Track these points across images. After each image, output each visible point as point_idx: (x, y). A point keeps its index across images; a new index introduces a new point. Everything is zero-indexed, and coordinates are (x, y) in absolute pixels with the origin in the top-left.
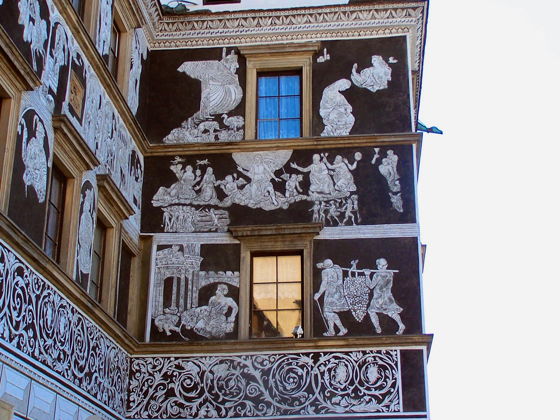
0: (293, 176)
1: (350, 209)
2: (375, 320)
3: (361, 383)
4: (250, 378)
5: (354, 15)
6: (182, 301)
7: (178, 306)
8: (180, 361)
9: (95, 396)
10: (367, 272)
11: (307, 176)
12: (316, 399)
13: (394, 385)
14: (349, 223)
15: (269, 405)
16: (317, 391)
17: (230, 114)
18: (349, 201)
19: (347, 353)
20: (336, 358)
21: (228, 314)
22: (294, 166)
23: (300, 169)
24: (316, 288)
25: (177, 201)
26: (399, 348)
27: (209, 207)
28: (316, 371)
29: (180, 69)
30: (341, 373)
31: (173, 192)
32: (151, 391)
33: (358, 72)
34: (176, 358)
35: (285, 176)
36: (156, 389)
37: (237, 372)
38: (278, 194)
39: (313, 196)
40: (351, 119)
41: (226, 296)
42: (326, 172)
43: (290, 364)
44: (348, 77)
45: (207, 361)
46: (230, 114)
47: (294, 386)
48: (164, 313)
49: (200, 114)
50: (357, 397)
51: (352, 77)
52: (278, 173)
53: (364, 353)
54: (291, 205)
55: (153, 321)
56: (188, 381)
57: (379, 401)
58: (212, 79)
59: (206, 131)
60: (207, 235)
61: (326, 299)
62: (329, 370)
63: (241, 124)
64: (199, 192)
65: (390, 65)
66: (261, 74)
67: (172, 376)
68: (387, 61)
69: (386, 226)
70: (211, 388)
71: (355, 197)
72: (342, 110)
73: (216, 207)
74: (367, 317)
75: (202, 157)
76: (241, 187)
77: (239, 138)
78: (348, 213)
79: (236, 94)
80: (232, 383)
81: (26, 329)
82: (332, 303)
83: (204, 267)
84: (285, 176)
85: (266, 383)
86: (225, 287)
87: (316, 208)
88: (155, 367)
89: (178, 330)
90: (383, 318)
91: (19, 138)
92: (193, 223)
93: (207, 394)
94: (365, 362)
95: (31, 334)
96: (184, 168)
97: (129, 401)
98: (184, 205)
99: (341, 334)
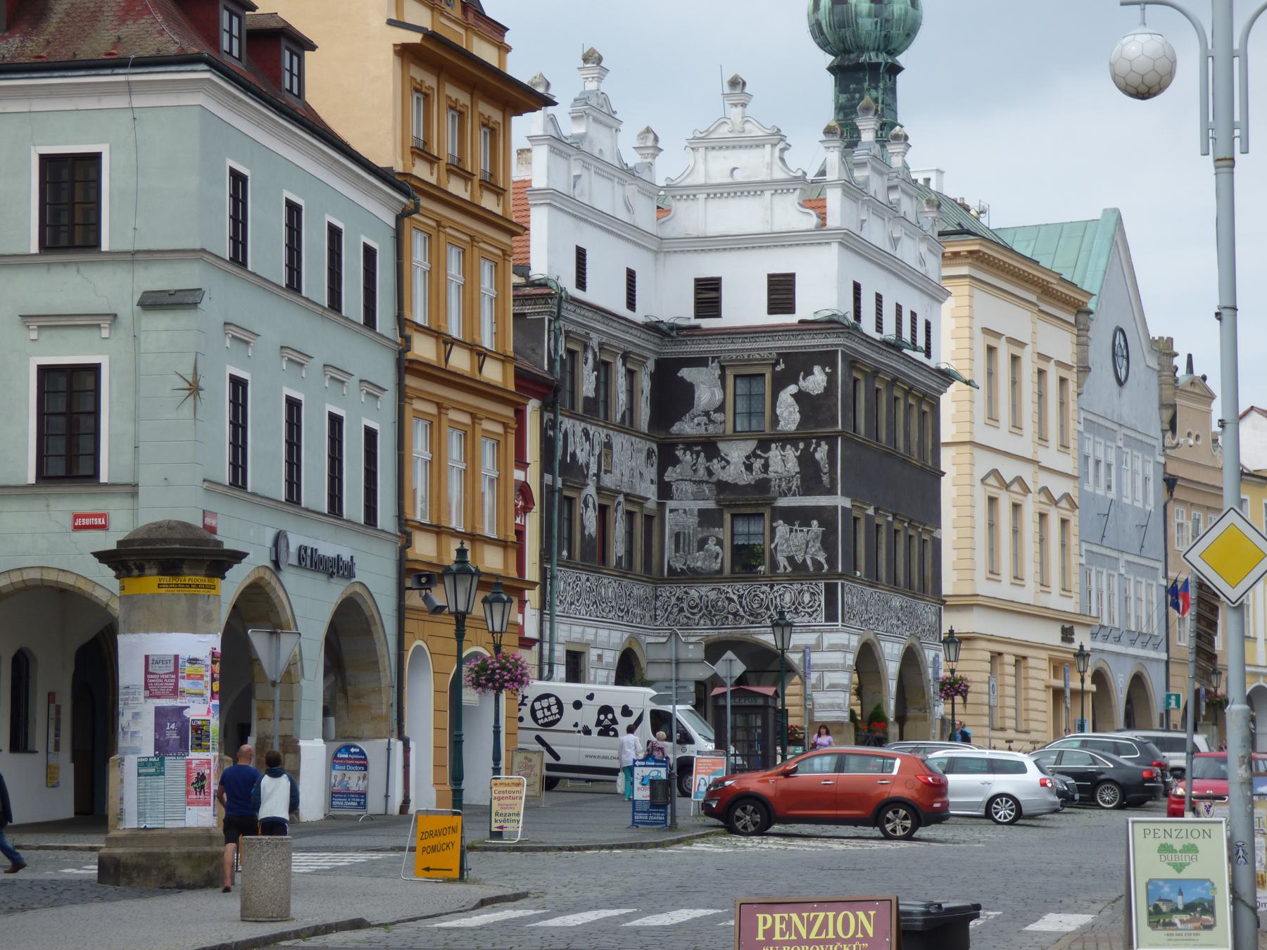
0: (758, 460)
1: (795, 485)
2: (809, 562)
3: (800, 605)
4: (730, 600)
5: (800, 337)
6: (687, 548)
7: (684, 551)
8: (686, 589)
9: (632, 622)
10: (805, 529)
11: (767, 459)
12: (772, 614)
13: (819, 606)
14: (794, 495)
15: (742, 617)
16: (772, 609)
17: (716, 411)
18: (795, 479)
19: (791, 584)
20: (784, 587)
21: (716, 558)
22: (759, 452)
23: (763, 455)
24: (772, 540)
25: (681, 478)
26: (823, 582)
27: (702, 482)
28: (772, 596)
29: (679, 374)
30: (787, 598)
31: (678, 471)
32: (669, 609)
33: (804, 379)
34: (684, 587)
35: (752, 460)
36: (672, 607)
37: (723, 596)
38: (748, 473)
39: (771, 475)
40: (797, 417)
41: (716, 545)
42: (780, 457)
43: (755, 591)
44: (796, 383)
45: (704, 589)
46: (716, 411)
47: (758, 605)
48: (676, 556)
49: (694, 411)
50: (797, 613)
51: (800, 384)
52: (748, 458)
53: (802, 584)
54: (756, 481)
55: (669, 562)
56: (692, 602)
57: (810, 616)
58: (702, 382)
59: (699, 424)
60: (701, 502)
61: (779, 548)
62: (780, 595)
63: (723, 419)
64: (695, 471)
65: (827, 374)
66: (736, 377)
67: (682, 599)
68: (824, 370)
69: (818, 497)
70: (707, 607)
71: (798, 475)
72: (792, 409)
73: (707, 482)
74: (804, 560)
75: (697, 444)
76: (723, 468)
77: (721, 431)
78: (794, 488)
79: (719, 395)
80: (720, 603)
82: (782, 551)
83: (700, 524)
84: (752, 460)
85: (741, 603)
86: (714, 538)
87: (773, 483)
88: (671, 593)
89: (685, 568)
90: (814, 561)
91: (582, 515)
92: (692, 493)
93: (704, 610)
94: (802, 590)
95: (595, 606)
96: (684, 453)
97: (656, 615)
98: (686, 480)
99: (788, 571)
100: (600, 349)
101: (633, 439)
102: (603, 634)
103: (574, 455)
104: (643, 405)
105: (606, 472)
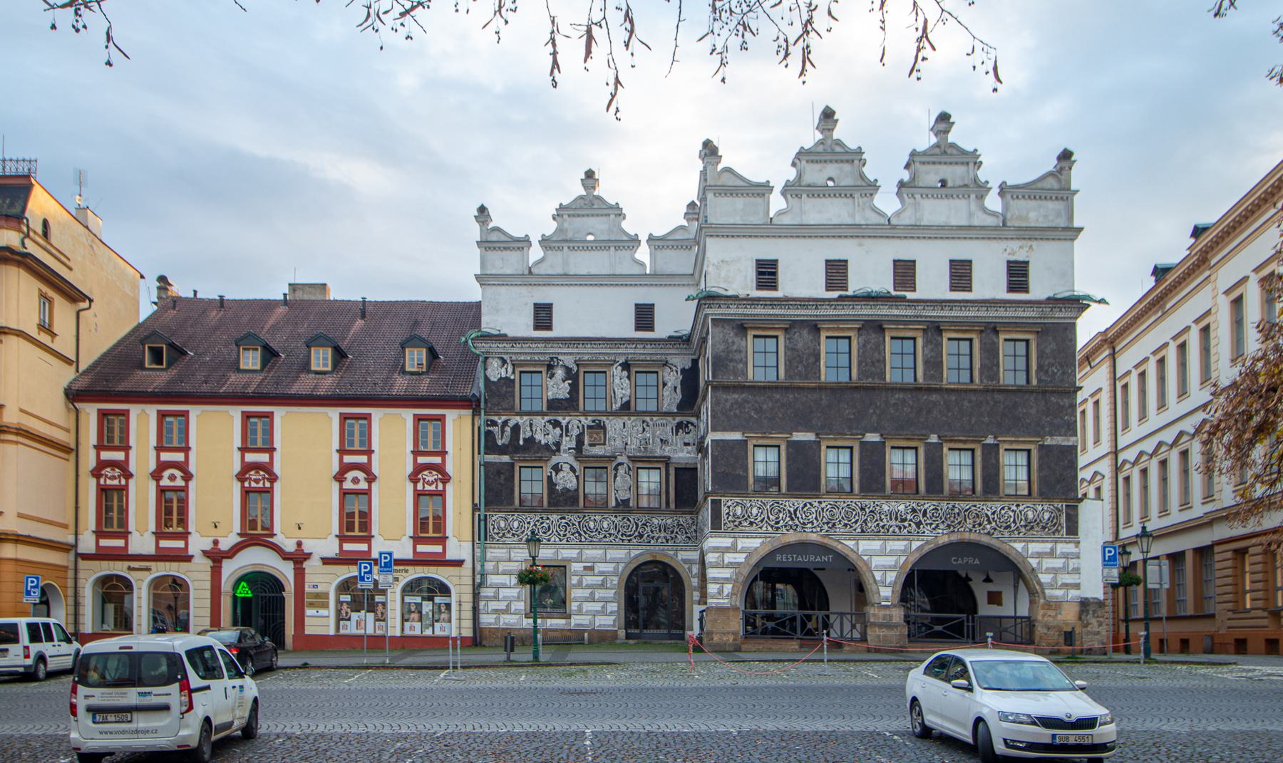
81: (572, 535)
100: (578, 365)
101: (648, 419)
102: (590, 553)
103: (530, 441)
104: (666, 393)
105: (591, 445)
